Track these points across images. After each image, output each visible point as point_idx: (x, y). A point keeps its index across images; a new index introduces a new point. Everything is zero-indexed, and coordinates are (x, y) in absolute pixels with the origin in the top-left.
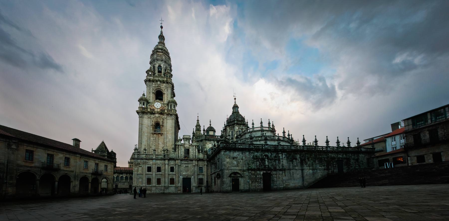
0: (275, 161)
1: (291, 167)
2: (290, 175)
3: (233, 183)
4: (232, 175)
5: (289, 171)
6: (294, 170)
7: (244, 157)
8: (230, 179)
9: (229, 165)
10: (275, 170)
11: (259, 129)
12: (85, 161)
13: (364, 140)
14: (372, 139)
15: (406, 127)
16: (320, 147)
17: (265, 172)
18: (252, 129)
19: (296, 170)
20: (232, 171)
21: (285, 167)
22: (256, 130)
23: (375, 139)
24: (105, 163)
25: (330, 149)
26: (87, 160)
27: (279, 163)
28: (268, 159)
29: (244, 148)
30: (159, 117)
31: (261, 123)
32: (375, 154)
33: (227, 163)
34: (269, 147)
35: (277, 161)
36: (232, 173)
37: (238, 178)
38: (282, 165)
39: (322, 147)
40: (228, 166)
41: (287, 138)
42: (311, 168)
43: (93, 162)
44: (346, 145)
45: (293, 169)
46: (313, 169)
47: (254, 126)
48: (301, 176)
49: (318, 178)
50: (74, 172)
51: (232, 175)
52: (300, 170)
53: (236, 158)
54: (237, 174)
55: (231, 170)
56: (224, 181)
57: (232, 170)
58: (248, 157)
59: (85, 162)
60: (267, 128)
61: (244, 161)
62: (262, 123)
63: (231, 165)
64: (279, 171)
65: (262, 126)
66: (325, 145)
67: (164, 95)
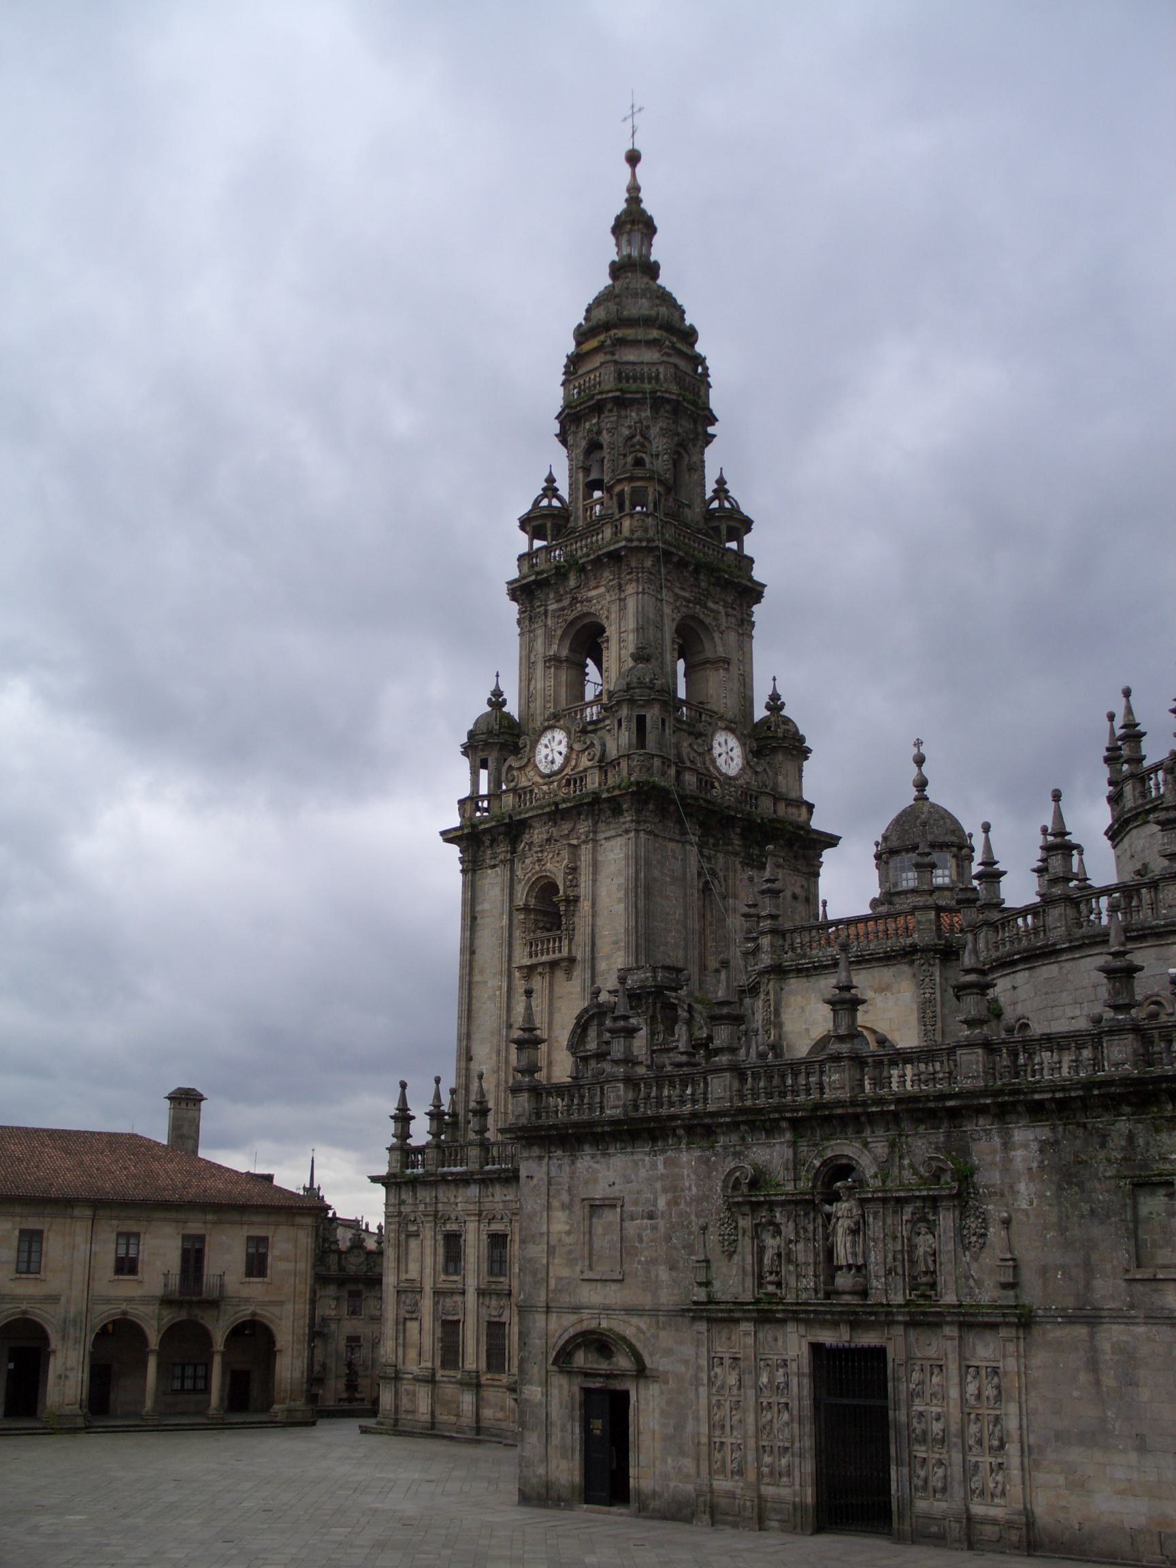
0: (926, 1222)
2: (1098, 1382)
4: (580, 1359)
5: (1082, 1331)
7: (665, 1191)
8: (566, 1386)
9: (565, 1272)
12: (119, 1234)
17: (828, 1337)
20: (581, 1321)
21: (1033, 1294)
24: (246, 1227)
26: (135, 1229)
30: (549, 840)
33: (551, 1251)
35: (946, 1220)
37: (618, 1385)
40: (559, 1279)
43: (169, 1229)
50: (63, 1299)
53: (615, 1206)
55: (576, 1309)
56: (526, 1399)
57: (585, 1314)
59: (122, 1241)
63: (578, 1268)
67: (605, 653)
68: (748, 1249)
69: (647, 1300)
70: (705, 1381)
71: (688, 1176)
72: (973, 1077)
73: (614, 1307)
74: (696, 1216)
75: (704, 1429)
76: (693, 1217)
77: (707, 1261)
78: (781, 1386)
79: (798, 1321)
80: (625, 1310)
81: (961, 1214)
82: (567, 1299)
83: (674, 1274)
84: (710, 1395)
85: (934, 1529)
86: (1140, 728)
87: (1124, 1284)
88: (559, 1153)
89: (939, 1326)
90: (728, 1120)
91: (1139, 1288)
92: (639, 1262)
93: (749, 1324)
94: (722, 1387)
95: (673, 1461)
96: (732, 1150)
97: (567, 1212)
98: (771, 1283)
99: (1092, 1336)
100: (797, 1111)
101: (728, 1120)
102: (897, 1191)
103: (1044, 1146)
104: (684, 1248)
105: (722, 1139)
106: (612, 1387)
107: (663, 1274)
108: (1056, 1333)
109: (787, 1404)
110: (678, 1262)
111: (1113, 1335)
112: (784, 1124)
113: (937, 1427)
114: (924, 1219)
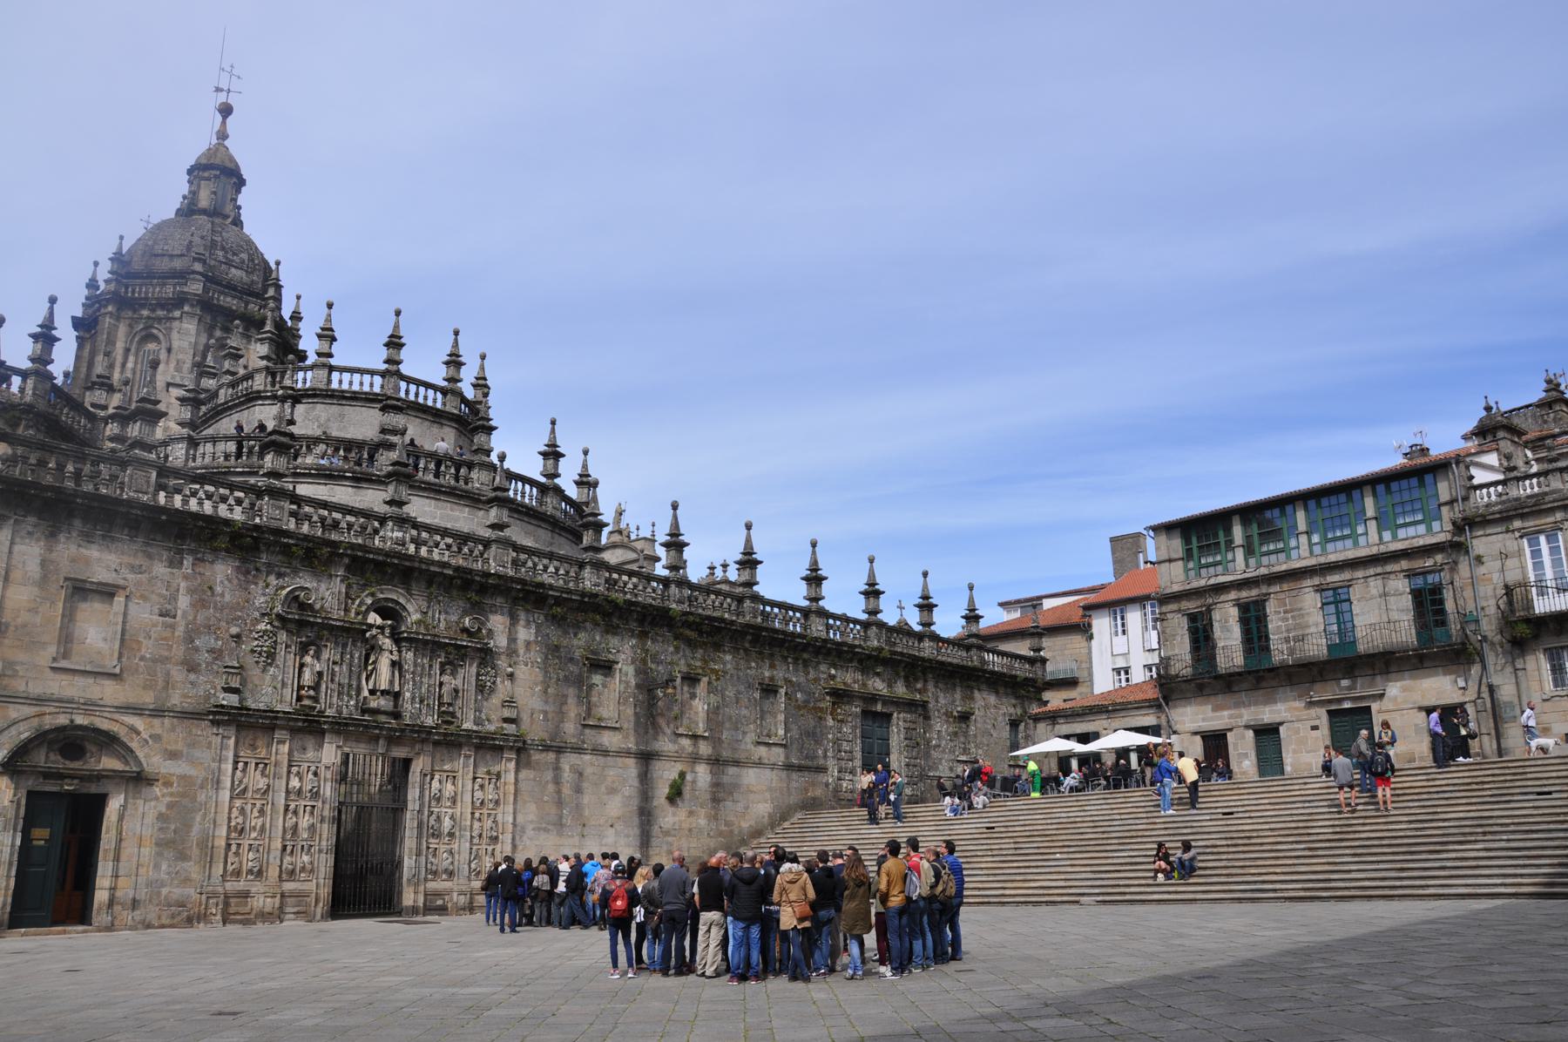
1: (570, 728)
2: (559, 792)
3: (41, 835)
4: (41, 758)
5: (551, 756)
6: (587, 757)
10: (449, 740)
11: (366, 388)
13: (1001, 605)
14: (1034, 603)
15: (1163, 565)
16: (773, 604)
18: (309, 374)
19: (605, 753)
22: (345, 386)
23: (1048, 604)
25: (828, 627)
27: (480, 688)
28: (397, 638)
29: (196, 516)
31: (395, 343)
32: (1047, 695)
34: (418, 542)
36: (42, 738)
37: (94, 789)
38: (509, 702)
39: (781, 605)
41: (568, 500)
42: (705, 749)
44: (914, 620)
45: (578, 750)
46: (716, 762)
47: (330, 355)
48: (635, 802)
49: (745, 825)
51: (41, 758)
52: (631, 762)
53: (112, 595)
54: (89, 747)
55: (39, 700)
58: (228, 598)
60: (431, 392)
61: (180, 631)
62: (402, 345)
64: (478, 747)
65: (392, 371)
66: (797, 595)
68: (290, 663)
69: (148, 699)
70: (229, 784)
71: (222, 582)
72: (504, 567)
73: (101, 703)
74: (228, 623)
75: (223, 832)
76: (223, 624)
77: (241, 667)
78: (315, 790)
79: (338, 733)
80: (116, 707)
81: (481, 664)
82: (22, 688)
83: (192, 677)
84: (231, 798)
85: (440, 902)
86: (462, 359)
87: (580, 727)
88: (32, 519)
89: (460, 746)
90: (291, 541)
91: (587, 731)
92: (142, 658)
93: (285, 732)
94: (245, 790)
95: (170, 866)
96: (276, 569)
97: (36, 590)
98: (309, 697)
99: (557, 760)
100: (369, 552)
101: (291, 541)
102: (444, 637)
103: (538, 627)
104: (208, 652)
105: (264, 558)
106: (84, 791)
107: (178, 674)
108: (536, 756)
109: (313, 807)
110: (199, 665)
111: (568, 761)
112: (346, 560)
113: (447, 823)
114: (450, 663)
